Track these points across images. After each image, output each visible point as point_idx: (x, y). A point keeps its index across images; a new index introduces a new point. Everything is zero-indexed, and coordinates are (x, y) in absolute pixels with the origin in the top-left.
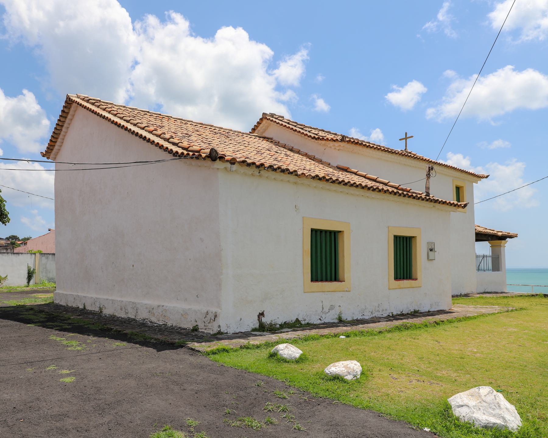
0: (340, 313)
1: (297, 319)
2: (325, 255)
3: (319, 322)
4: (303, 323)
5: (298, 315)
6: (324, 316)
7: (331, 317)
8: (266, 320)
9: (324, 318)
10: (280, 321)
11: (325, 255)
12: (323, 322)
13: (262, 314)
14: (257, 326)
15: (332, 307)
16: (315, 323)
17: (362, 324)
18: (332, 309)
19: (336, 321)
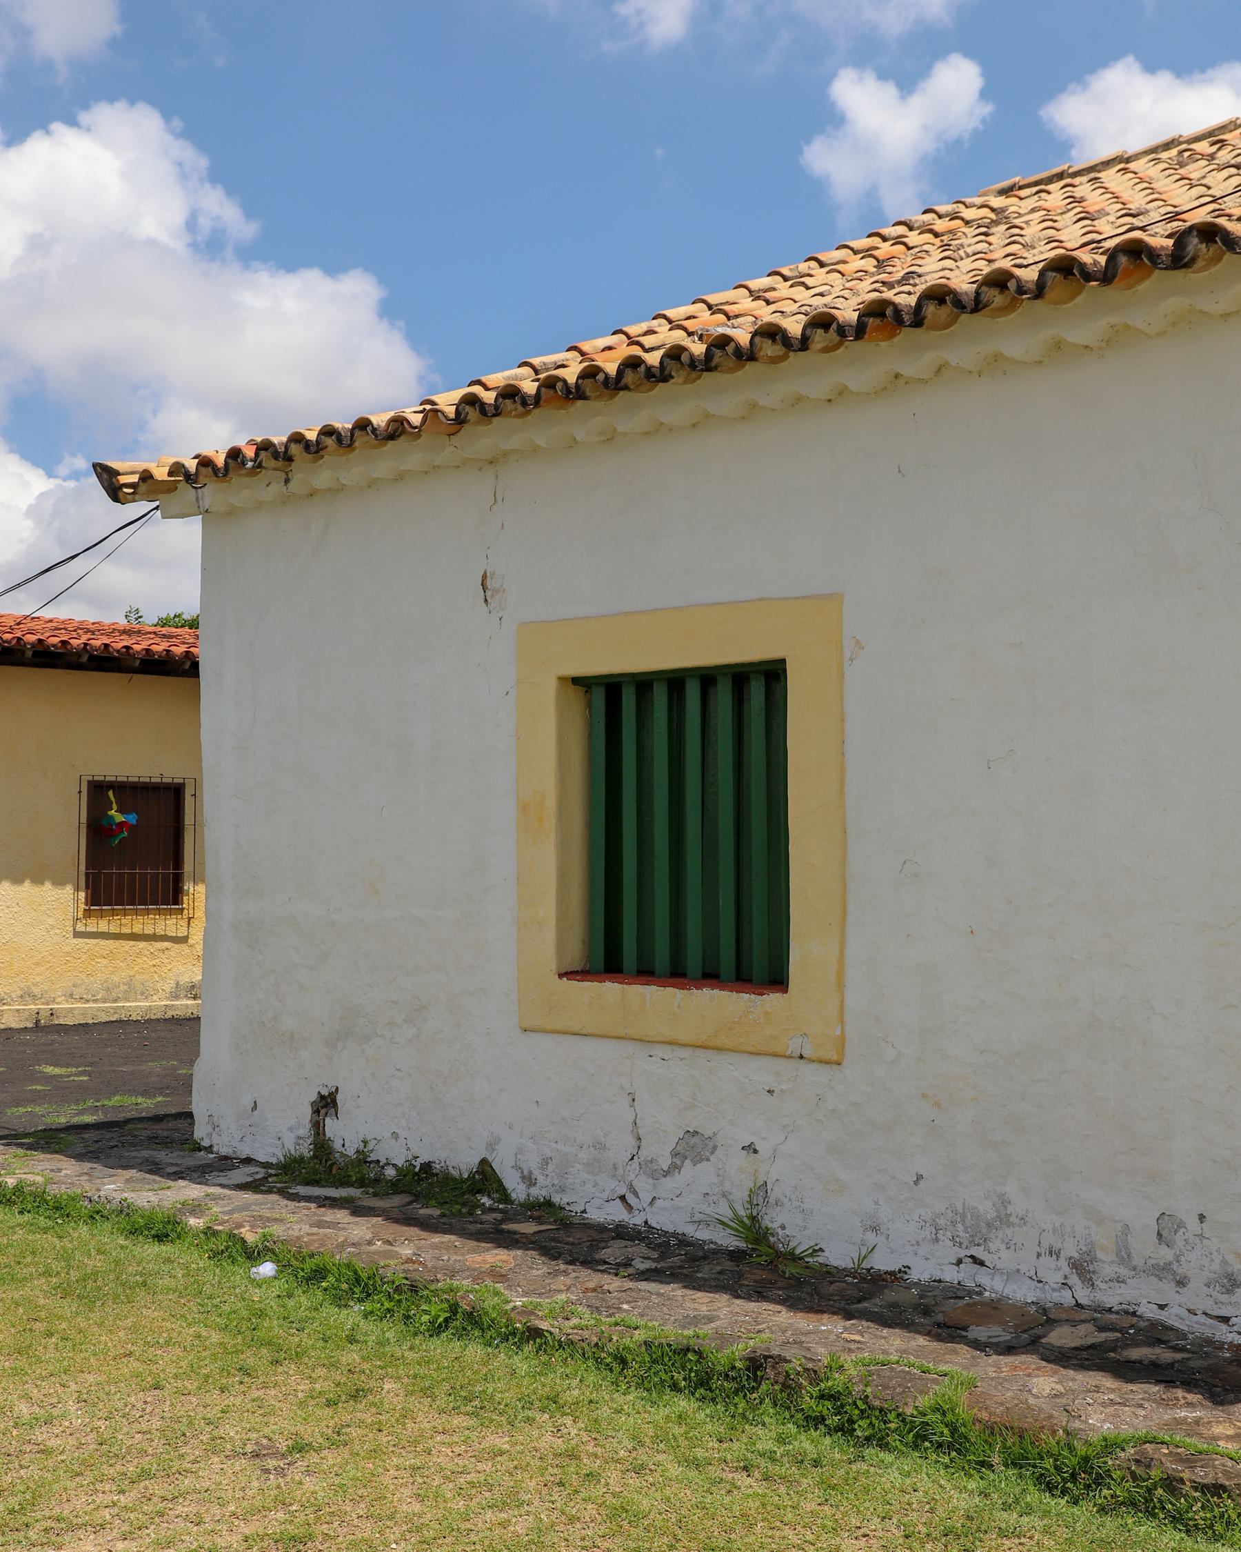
0: (760, 1192)
1: (484, 1162)
2: (683, 818)
3: (615, 1214)
4: (518, 1191)
5: (491, 1146)
6: (643, 1185)
7: (686, 1205)
8: (345, 1133)
9: (646, 1197)
10: (394, 1153)
11: (683, 818)
12: (637, 1220)
13: (326, 1104)
14: (306, 1150)
15: (693, 1147)
16: (597, 1215)
17: (793, 1304)
18: (698, 1159)
19: (728, 1240)
